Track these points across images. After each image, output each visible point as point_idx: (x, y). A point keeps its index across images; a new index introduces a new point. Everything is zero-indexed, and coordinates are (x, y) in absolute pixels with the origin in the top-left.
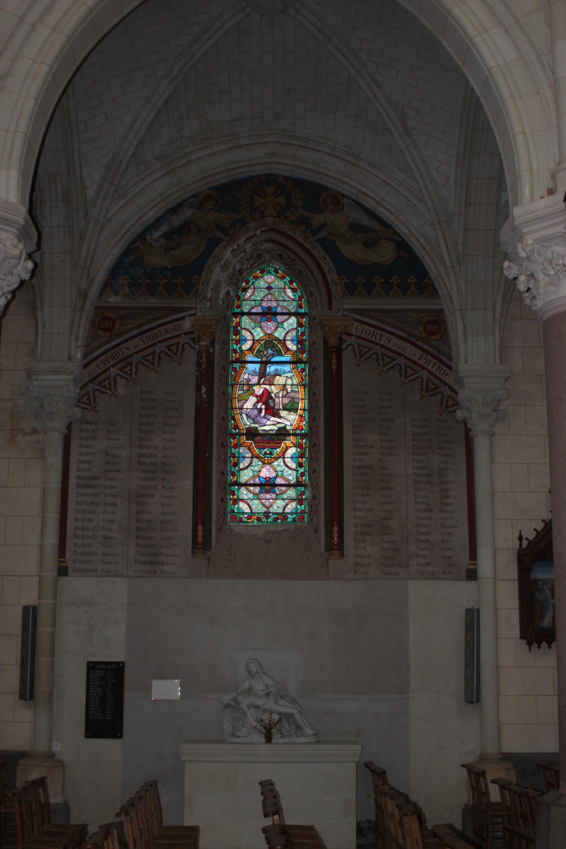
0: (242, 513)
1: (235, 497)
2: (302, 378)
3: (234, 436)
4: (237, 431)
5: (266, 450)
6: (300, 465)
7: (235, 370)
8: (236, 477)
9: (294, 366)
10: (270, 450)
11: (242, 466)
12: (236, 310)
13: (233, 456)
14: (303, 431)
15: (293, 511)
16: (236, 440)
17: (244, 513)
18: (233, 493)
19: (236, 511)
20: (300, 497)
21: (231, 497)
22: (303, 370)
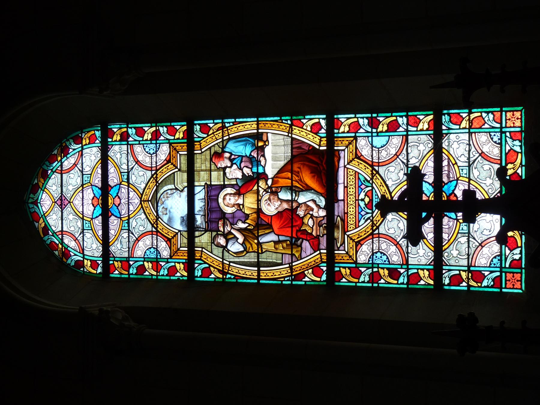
0: (501, 260)
1: (464, 275)
2: (218, 130)
3: (334, 276)
4: (325, 269)
5: (362, 204)
6: (393, 127)
7: (206, 272)
8: (421, 272)
9: (197, 146)
10: (362, 196)
11: (396, 259)
12: (99, 270)
13: (375, 277)
14: (323, 123)
15: (496, 139)
16: (343, 270)
17: (501, 255)
18: (456, 280)
19: (498, 274)
20: (464, 124)
21: (464, 284)
22: (205, 129)
